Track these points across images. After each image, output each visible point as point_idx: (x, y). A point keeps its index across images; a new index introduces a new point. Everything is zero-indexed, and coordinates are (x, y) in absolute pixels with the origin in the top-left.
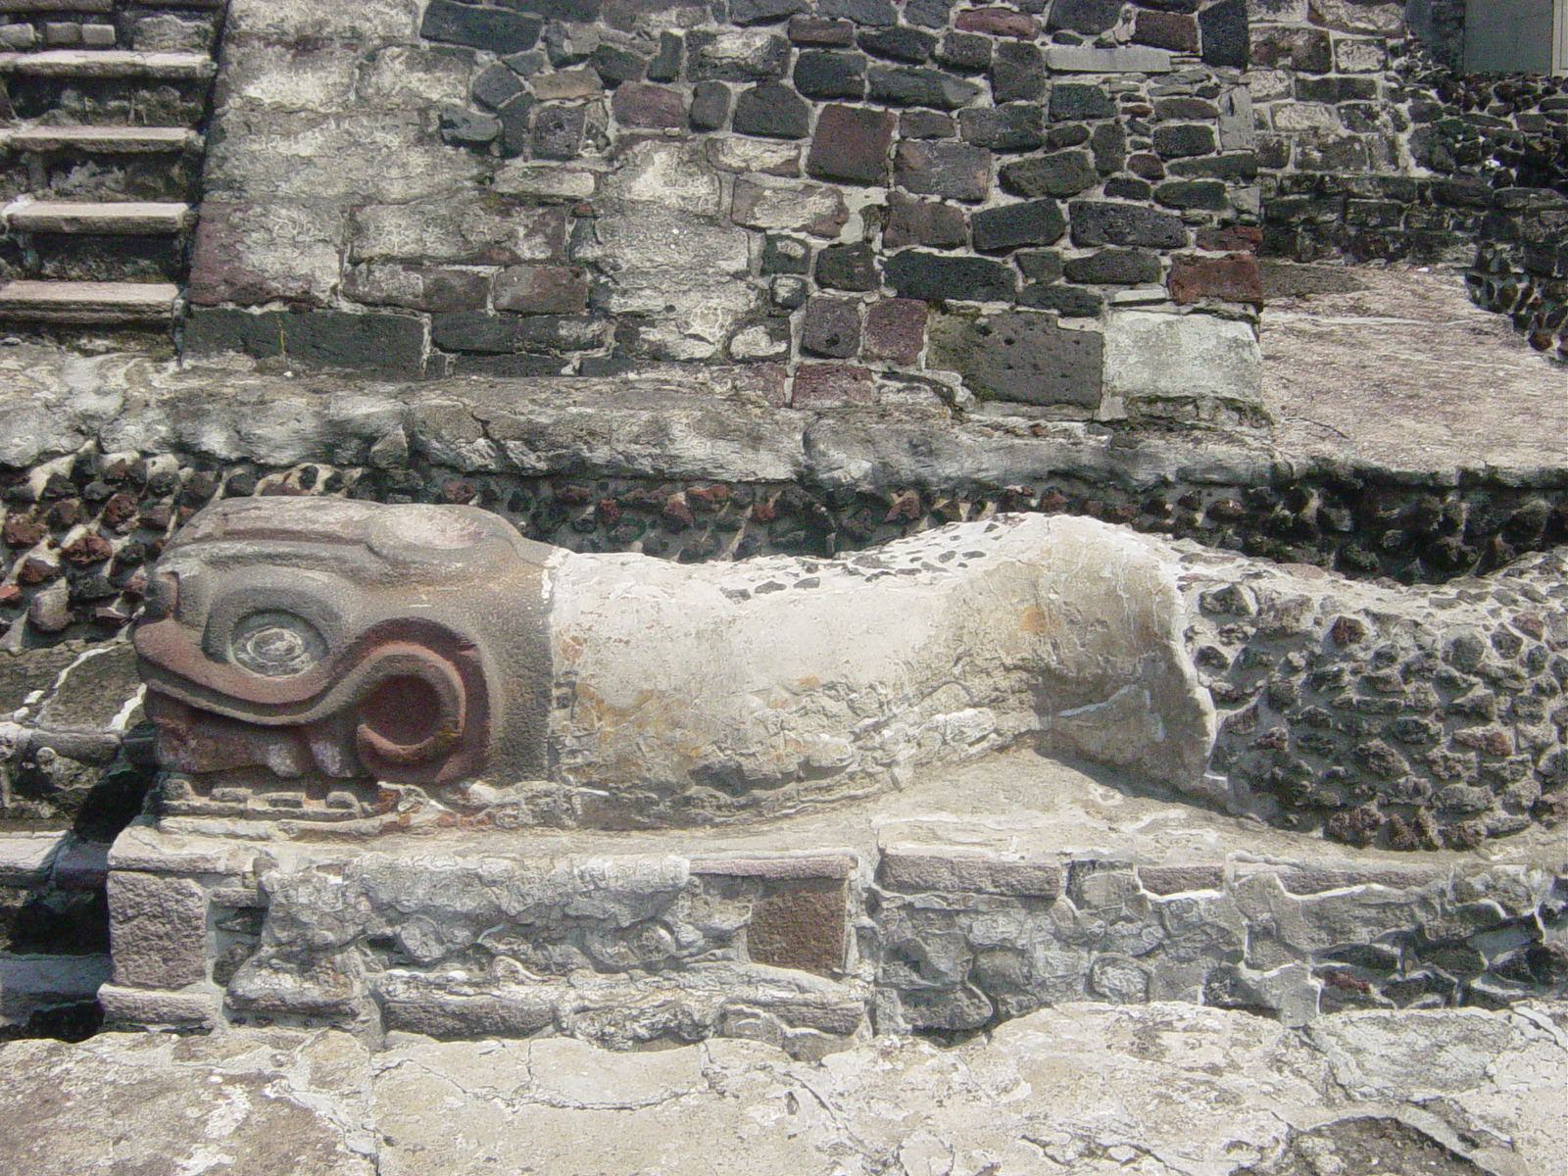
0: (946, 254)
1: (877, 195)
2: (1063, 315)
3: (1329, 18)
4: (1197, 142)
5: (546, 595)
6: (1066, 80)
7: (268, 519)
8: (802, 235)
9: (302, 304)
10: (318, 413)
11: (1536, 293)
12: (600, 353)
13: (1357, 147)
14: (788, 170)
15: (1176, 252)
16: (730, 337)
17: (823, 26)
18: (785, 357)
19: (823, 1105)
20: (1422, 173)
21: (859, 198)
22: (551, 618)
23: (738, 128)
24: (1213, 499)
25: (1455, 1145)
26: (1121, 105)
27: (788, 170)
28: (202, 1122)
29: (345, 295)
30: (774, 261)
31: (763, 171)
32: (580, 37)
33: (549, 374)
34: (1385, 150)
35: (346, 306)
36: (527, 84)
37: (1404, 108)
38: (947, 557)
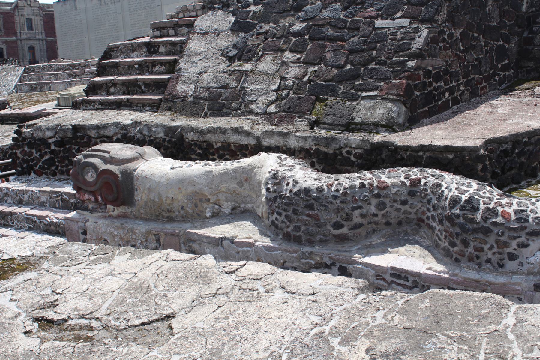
2: (349, 100)
14: (298, 61)
23: (291, 51)
27: (298, 61)
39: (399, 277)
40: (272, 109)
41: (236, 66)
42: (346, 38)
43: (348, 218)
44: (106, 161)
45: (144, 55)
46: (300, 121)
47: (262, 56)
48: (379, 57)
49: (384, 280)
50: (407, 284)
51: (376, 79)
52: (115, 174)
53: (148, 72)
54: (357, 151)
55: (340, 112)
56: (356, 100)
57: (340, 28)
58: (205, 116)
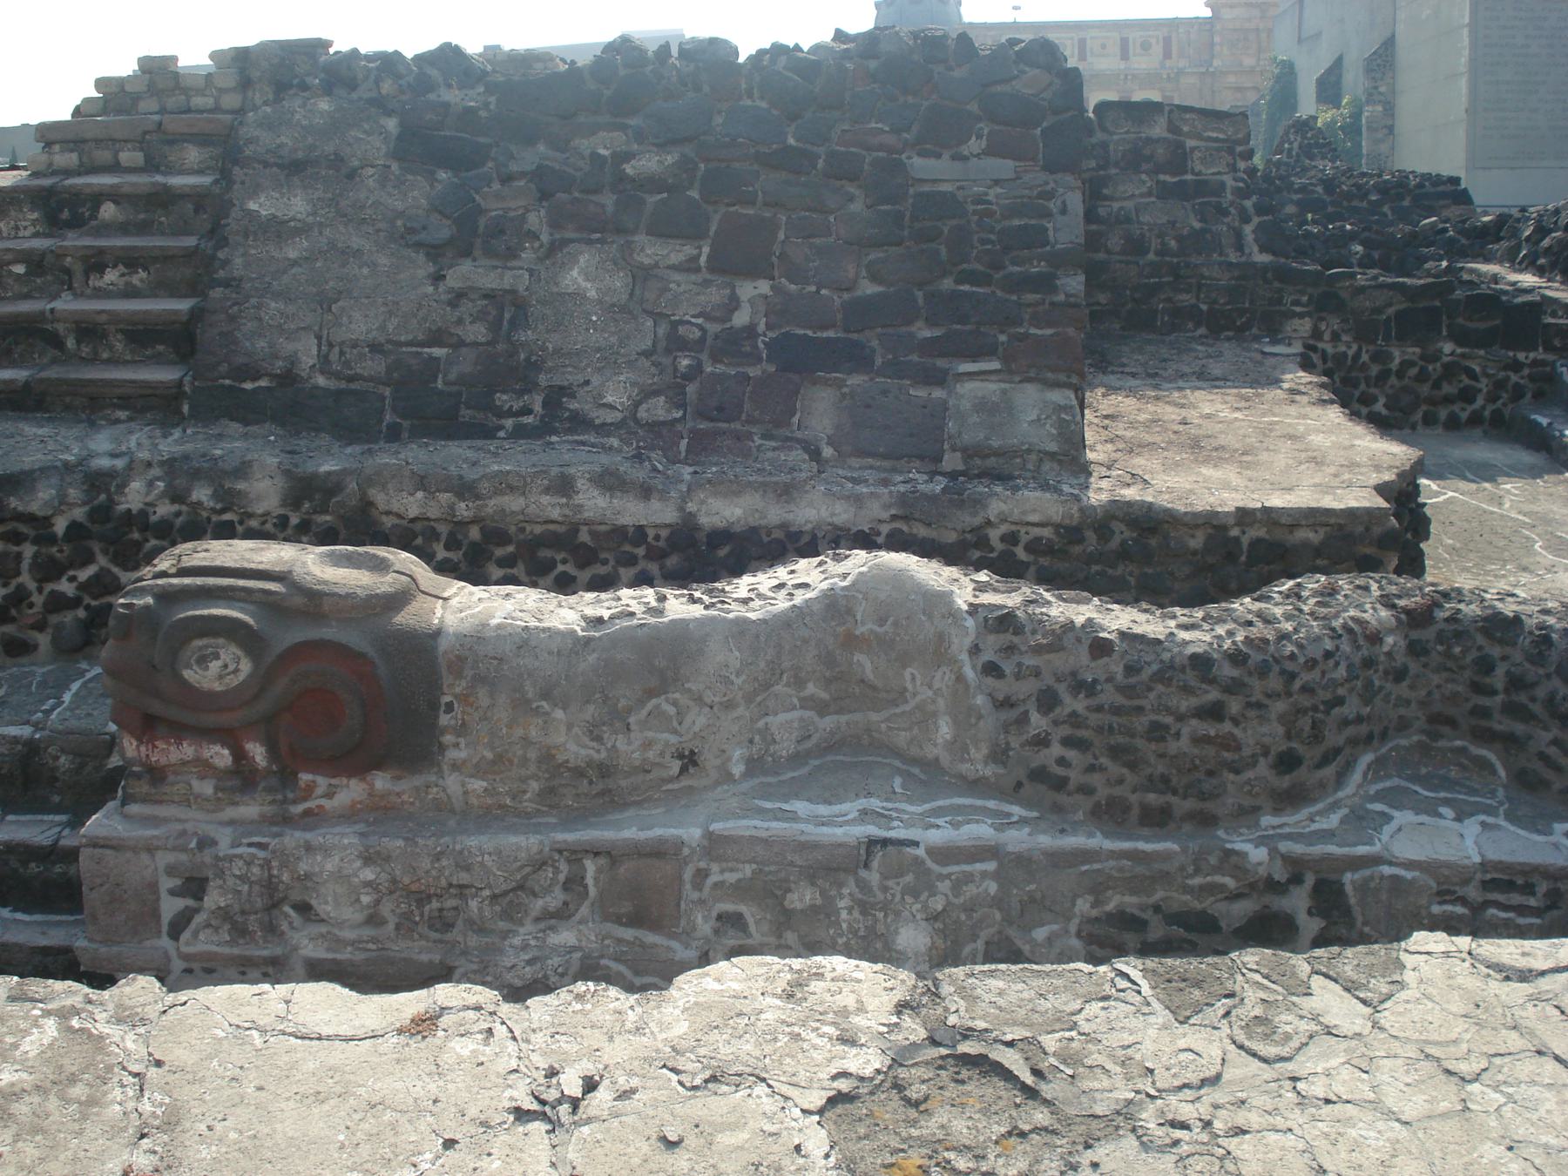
0: (819, 334)
1: (764, 287)
3: (1186, 129)
4: (1034, 238)
6: (926, 188)
7: (213, 559)
8: (700, 321)
10: (289, 471)
11: (1365, 357)
12: (528, 420)
13: (1208, 236)
14: (690, 266)
15: (1012, 330)
16: (637, 405)
19: (514, 1038)
20: (1262, 258)
22: (439, 640)
23: (650, 232)
25: (1028, 1079)
26: (971, 208)
27: (690, 266)
28: (16, 1046)
29: (322, 372)
30: (677, 344)
31: (669, 267)
33: (486, 438)
35: (321, 381)
36: (477, 198)
37: (1248, 204)
38: (781, 586)
39: (1509, 886)
40: (658, 409)
41: (463, 273)
43: (1316, 737)
45: (31, 230)
46: (774, 449)
49: (1463, 901)
50: (1532, 902)
52: (362, 655)
53: (70, 288)
54: (1037, 531)
58: (394, 435)
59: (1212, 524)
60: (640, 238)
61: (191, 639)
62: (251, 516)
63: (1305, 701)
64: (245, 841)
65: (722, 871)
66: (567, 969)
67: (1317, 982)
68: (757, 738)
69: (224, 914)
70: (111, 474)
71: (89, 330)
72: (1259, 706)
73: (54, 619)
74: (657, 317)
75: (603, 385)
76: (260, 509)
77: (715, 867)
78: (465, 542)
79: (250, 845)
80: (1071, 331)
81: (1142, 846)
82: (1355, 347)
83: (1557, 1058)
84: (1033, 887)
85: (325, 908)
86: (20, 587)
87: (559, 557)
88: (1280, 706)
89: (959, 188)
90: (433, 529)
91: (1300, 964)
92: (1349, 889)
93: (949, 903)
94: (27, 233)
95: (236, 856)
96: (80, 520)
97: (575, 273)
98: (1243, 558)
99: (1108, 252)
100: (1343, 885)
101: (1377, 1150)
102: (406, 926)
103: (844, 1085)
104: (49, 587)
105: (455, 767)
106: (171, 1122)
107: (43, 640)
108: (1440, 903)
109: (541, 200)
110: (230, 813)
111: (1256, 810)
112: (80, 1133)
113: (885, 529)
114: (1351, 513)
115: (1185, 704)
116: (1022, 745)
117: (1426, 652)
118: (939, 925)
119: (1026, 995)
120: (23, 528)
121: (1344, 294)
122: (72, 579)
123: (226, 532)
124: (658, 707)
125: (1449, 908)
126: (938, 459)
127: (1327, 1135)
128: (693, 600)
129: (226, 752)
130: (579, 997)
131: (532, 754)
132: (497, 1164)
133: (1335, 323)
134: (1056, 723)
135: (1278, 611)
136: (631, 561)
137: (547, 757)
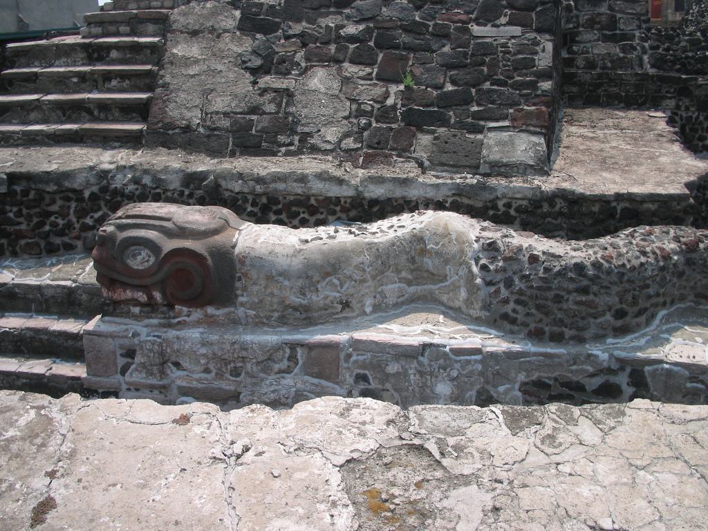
2: (470, 132)
3: (617, 9)
4: (529, 64)
5: (234, 240)
7: (141, 211)
9: (187, 129)
11: (701, 118)
12: (292, 148)
13: (626, 60)
14: (368, 77)
15: (516, 108)
16: (340, 141)
17: (388, 21)
18: (361, 148)
19: (221, 427)
20: (652, 71)
21: (393, 89)
23: (352, 62)
24: (517, 205)
25: (437, 456)
27: (368, 77)
28: (17, 421)
32: (297, 28)
33: (273, 156)
34: (638, 62)
35: (201, 130)
36: (274, 46)
37: (646, 45)
38: (392, 226)
40: (350, 143)
41: (267, 80)
42: (434, 48)
43: (634, 303)
44: (169, 234)
45: (81, 62)
46: (402, 162)
47: (307, 69)
48: (493, 75)
51: (500, 104)
54: (521, 202)
55: (464, 149)
56: (481, 132)
57: (420, 34)
58: (233, 154)
59: (602, 200)
60: (346, 65)
61: (129, 246)
62: (168, 190)
63: (627, 286)
64: (152, 334)
65: (358, 355)
66: (289, 395)
67: (582, 420)
68: (378, 296)
69: (143, 365)
70: (109, 171)
71: (104, 106)
72: (607, 288)
73: (84, 234)
74: (353, 101)
75: (326, 132)
76: (172, 187)
77: (355, 354)
78: (260, 203)
79: (154, 336)
80: (544, 108)
81: (549, 350)
82: (696, 114)
83: (686, 462)
84: (498, 367)
85: (185, 364)
86: (70, 221)
87: (301, 210)
88: (615, 289)
89: (494, 40)
90: (246, 197)
91: (576, 410)
92: (647, 374)
93: (460, 373)
94: (79, 64)
95: (147, 341)
96: (94, 191)
97: (316, 81)
98: (618, 216)
99: (578, 68)
100: (644, 372)
101: (586, 499)
102: (220, 375)
103: (355, 455)
104: (81, 221)
105: (242, 304)
106: (72, 455)
107: (79, 244)
108: (691, 382)
109: (302, 47)
110: (147, 321)
111: (604, 336)
112: (35, 458)
113: (450, 200)
114: (671, 197)
115: (572, 286)
116: (497, 303)
117: (694, 263)
118: (455, 383)
119: (447, 419)
120: (71, 195)
121: (691, 88)
122: (92, 217)
123: (157, 198)
124: (331, 281)
125: (695, 385)
126: (477, 167)
127: (565, 490)
128: (351, 232)
129: (145, 296)
130: (252, 411)
131: (275, 300)
132: (200, 480)
133: (687, 101)
134: (512, 293)
135: (621, 243)
136: (334, 213)
137: (282, 302)
